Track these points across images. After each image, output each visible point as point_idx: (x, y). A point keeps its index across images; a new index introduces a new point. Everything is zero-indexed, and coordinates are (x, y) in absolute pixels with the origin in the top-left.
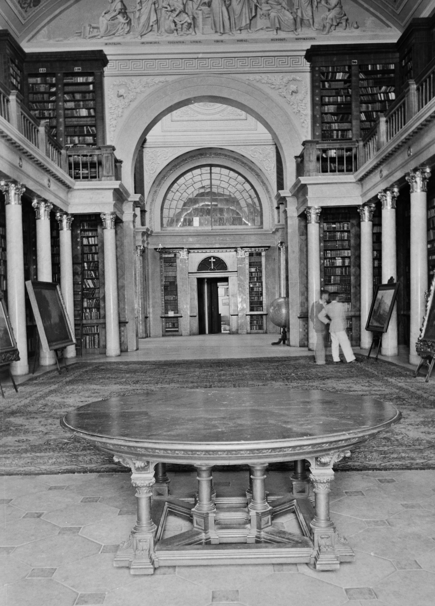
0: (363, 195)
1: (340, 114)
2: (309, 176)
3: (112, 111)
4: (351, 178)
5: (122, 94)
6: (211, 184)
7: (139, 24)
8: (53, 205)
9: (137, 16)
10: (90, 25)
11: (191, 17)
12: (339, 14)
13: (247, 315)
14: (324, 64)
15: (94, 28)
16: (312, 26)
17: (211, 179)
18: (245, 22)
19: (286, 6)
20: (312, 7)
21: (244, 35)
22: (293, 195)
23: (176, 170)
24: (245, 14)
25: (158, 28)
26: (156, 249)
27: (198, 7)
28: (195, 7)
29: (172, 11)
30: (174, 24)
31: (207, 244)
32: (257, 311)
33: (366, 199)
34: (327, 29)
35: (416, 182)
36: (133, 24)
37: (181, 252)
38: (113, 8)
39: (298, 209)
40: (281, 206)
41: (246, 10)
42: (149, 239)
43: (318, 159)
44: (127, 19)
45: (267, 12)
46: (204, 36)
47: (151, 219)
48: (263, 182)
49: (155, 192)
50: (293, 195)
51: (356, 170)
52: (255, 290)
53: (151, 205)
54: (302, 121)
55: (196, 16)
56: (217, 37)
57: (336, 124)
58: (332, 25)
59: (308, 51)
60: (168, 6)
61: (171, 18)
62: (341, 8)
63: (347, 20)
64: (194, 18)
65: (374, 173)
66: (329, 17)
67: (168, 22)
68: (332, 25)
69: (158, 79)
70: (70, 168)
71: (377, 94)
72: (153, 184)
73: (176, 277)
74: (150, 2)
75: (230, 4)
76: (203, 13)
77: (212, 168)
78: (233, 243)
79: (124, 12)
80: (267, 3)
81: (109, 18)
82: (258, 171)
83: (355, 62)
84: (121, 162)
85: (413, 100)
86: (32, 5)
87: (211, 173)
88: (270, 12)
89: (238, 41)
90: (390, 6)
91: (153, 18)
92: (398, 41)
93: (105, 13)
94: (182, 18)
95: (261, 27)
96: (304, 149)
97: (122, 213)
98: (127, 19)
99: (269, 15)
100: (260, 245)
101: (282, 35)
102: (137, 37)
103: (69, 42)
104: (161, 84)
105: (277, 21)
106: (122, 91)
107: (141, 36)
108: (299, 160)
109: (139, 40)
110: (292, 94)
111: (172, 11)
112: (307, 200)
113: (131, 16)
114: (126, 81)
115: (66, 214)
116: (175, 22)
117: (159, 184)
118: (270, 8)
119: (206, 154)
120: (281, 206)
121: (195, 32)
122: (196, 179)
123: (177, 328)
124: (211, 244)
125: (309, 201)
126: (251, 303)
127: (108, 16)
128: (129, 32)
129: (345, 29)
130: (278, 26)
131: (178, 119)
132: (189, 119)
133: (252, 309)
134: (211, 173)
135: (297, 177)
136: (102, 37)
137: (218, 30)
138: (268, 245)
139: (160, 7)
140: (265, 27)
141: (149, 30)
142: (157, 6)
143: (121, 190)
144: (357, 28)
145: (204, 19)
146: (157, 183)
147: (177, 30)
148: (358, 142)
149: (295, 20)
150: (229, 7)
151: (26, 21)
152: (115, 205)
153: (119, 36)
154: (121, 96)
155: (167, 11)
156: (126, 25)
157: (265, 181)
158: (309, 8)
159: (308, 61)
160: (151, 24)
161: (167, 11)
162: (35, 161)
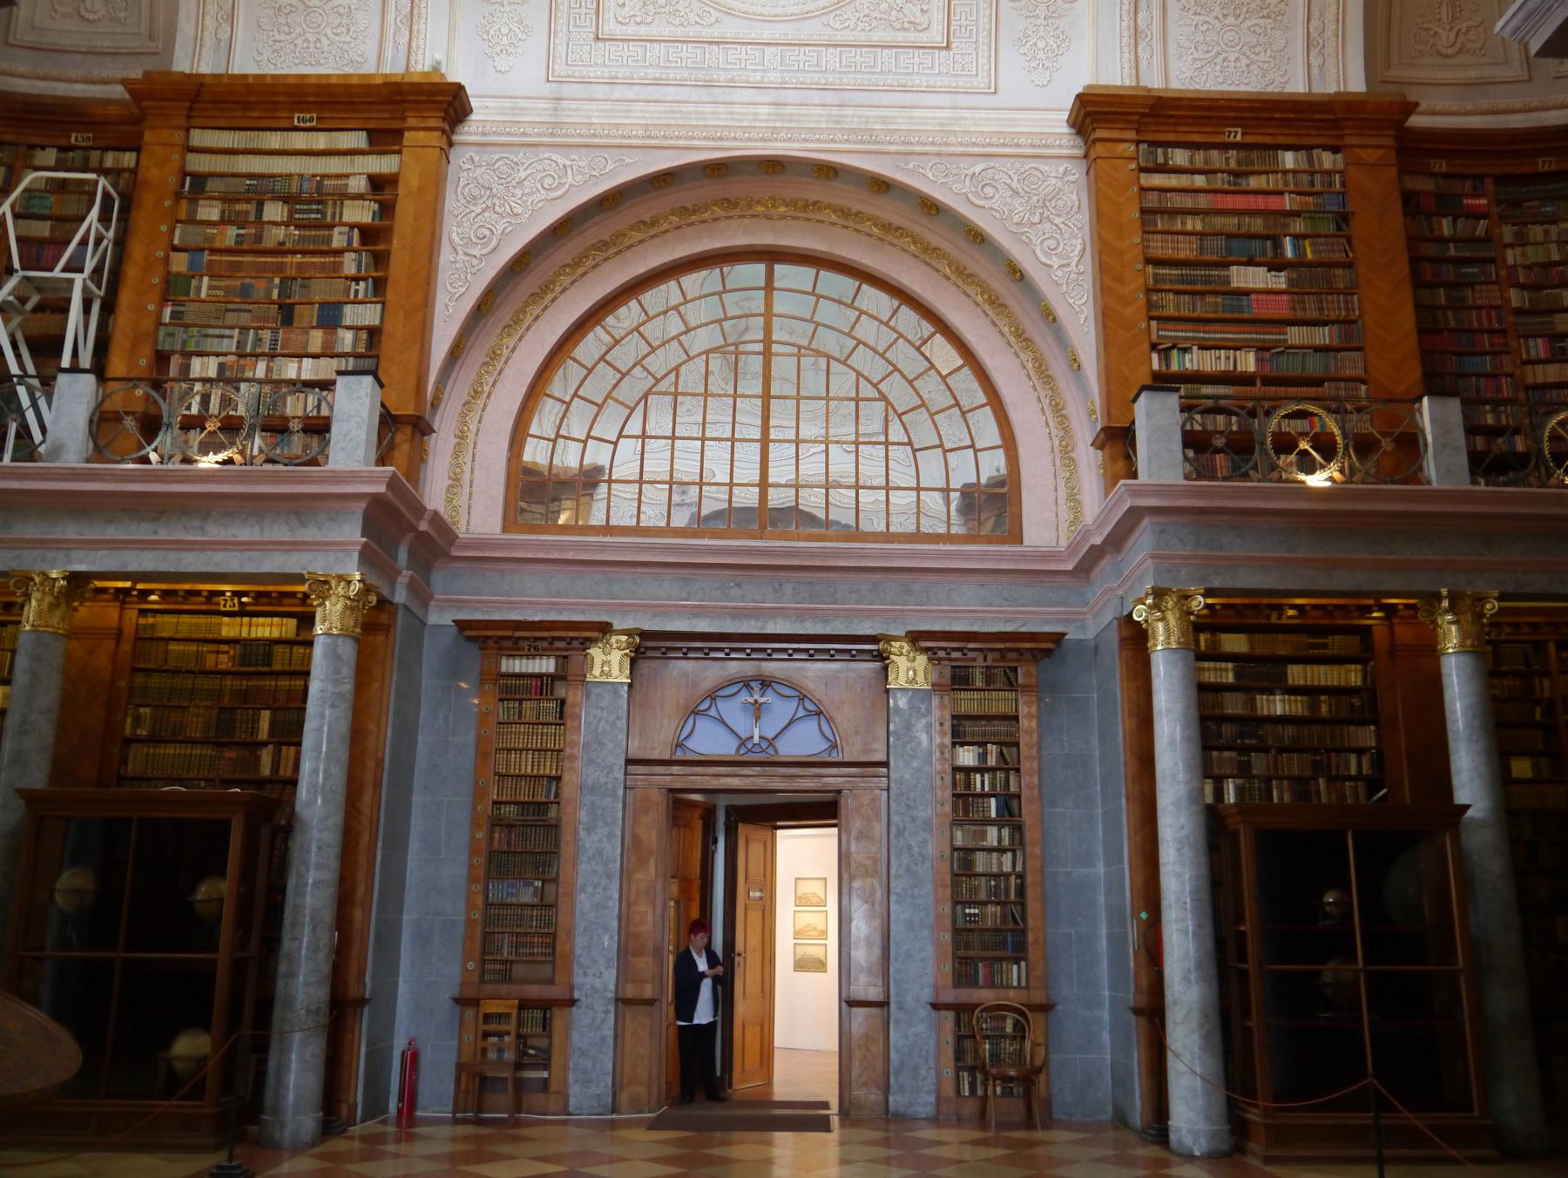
6: (768, 341)
13: (936, 1006)
17: (768, 314)
23: (605, 267)
26: (461, 625)
31: (736, 614)
32: (991, 984)
37: (595, 652)
42: (439, 579)
47: (456, 479)
48: (1019, 334)
49: (494, 356)
52: (981, 863)
73: (558, 779)
77: (780, 269)
78: (871, 614)
87: (769, 287)
100: (1009, 628)
117: (517, 322)
123: (546, 1067)
124: (757, 613)
126: (962, 934)
131: (630, 30)
132: (680, 32)
133: (964, 973)
138: (1047, 629)
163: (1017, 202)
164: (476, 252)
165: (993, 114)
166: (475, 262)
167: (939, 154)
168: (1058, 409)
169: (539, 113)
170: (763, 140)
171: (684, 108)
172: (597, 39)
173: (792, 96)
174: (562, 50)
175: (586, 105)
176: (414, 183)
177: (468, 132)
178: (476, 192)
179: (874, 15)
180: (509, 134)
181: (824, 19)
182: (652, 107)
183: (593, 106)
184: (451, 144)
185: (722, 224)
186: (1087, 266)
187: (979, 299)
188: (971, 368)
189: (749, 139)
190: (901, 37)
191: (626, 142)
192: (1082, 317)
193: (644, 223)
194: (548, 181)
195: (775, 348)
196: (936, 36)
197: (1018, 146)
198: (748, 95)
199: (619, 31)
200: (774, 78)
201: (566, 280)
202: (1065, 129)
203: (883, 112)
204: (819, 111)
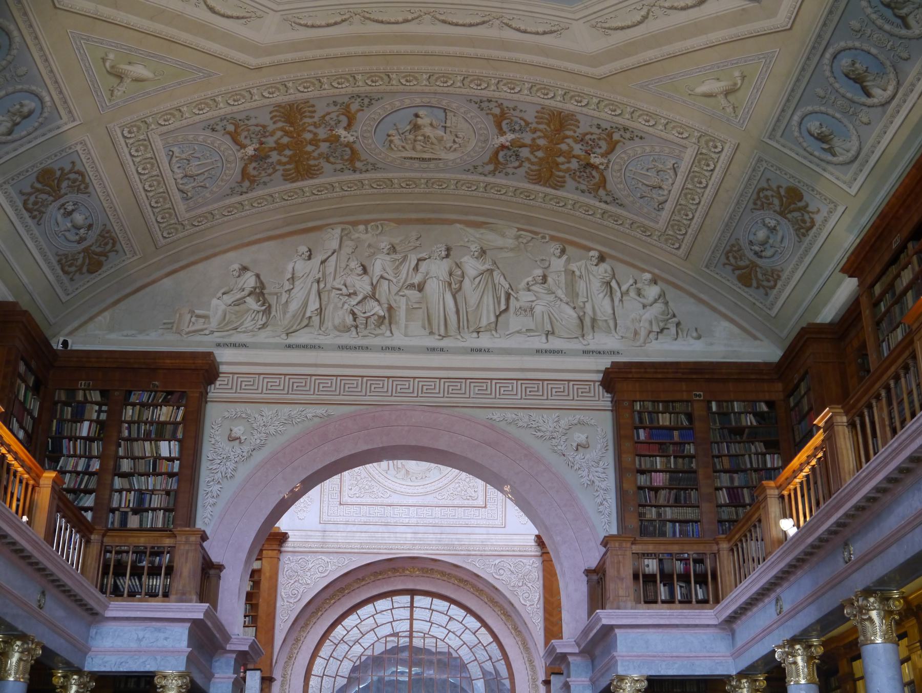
0: (736, 655)
1: (672, 489)
2: (619, 608)
3: (214, 467)
4: (709, 616)
5: (238, 436)
6: (411, 630)
7: (285, 313)
8: (44, 648)
9: (284, 300)
10: (192, 312)
11: (386, 306)
12: (663, 313)
14: (638, 397)
15: (198, 316)
16: (613, 331)
17: (411, 619)
18: (487, 318)
19: (563, 296)
20: (612, 300)
21: (484, 341)
22: (581, 653)
23: (343, 600)
24: (488, 305)
25: (322, 323)
27: (399, 291)
28: (394, 289)
29: (349, 295)
30: (351, 316)
33: (744, 662)
34: (642, 340)
35: (870, 619)
36: (273, 313)
38: (240, 286)
39: (593, 682)
40: (552, 678)
41: (488, 300)
43: (636, 577)
44: (263, 305)
45: (529, 304)
46: (406, 338)
48: (516, 628)
49: (297, 640)
50: (581, 653)
51: (717, 601)
53: (285, 668)
54: (599, 500)
55: (394, 305)
56: (432, 342)
57: (668, 509)
58: (650, 332)
59: (607, 373)
60: (343, 287)
61: (346, 306)
62: (666, 303)
63: (678, 324)
64: (390, 309)
65: (761, 605)
66: (644, 317)
67: (340, 313)
68: (650, 332)
69: (311, 411)
70: (105, 573)
71: (743, 455)
72: (293, 624)
74: (311, 279)
75: (460, 289)
76: (408, 299)
77: (416, 598)
79: (259, 292)
80: (529, 290)
81: (229, 302)
82: (508, 608)
83: (699, 395)
84: (220, 567)
85: (843, 447)
86: (85, 269)
87: (412, 607)
88: (534, 304)
89: (472, 350)
90: (758, 304)
91: (313, 305)
92: (784, 357)
93: (224, 294)
94: (367, 308)
95: (517, 329)
96: (605, 554)
97: (209, 676)
98: (263, 305)
99: (532, 309)
101: (555, 343)
102: (279, 336)
103: (147, 338)
104: (317, 420)
105: (546, 317)
106: (238, 431)
107: (287, 334)
108: (595, 577)
109: (283, 340)
110: (577, 450)
111: (349, 295)
112: (616, 662)
113: (272, 300)
114: (249, 412)
115: (79, 672)
116: (354, 314)
117: (306, 625)
118: (534, 298)
119: (404, 569)
120: (552, 678)
121: (391, 333)
122: (380, 619)
125: (619, 663)
127: (229, 299)
128: (264, 326)
129: (676, 339)
130: (550, 329)
131: (354, 500)
132: (375, 501)
134: (412, 607)
135: (591, 611)
136: (212, 332)
137: (435, 330)
139: (329, 286)
140: (524, 330)
141: (305, 322)
142: (322, 285)
143: (209, 624)
144: (699, 337)
145: (410, 310)
146: (301, 622)
147: (356, 327)
148: (717, 544)
149: (581, 320)
150: (457, 292)
151: (69, 297)
152: (190, 659)
153: (244, 332)
154: (237, 439)
155: (342, 295)
156: (261, 314)
157: (521, 628)
158: (607, 302)
159: (607, 392)
160: (308, 314)
161: (342, 295)
162: (9, 543)
163: (513, 576)
164: (292, 601)
165: (504, 537)
166: (291, 605)
167: (481, 555)
168: (531, 662)
169: (317, 537)
170: (409, 549)
171: (376, 535)
172: (341, 504)
173: (421, 529)
174: (326, 509)
175: (336, 534)
176: (268, 574)
177: (288, 546)
178: (291, 574)
179: (455, 493)
180: (305, 547)
181: (434, 495)
182: (363, 535)
183: (339, 534)
184: (280, 552)
185: (392, 579)
186: (541, 605)
187: (499, 613)
188: (496, 643)
189: (403, 549)
190: (466, 503)
191: (353, 550)
192: (538, 628)
193: (359, 579)
194: (321, 569)
195: (415, 634)
196: (480, 502)
197: (514, 551)
198: (403, 529)
199: (349, 500)
200: (413, 521)
201: (327, 607)
202: (534, 544)
203: (459, 536)
204: (431, 536)
